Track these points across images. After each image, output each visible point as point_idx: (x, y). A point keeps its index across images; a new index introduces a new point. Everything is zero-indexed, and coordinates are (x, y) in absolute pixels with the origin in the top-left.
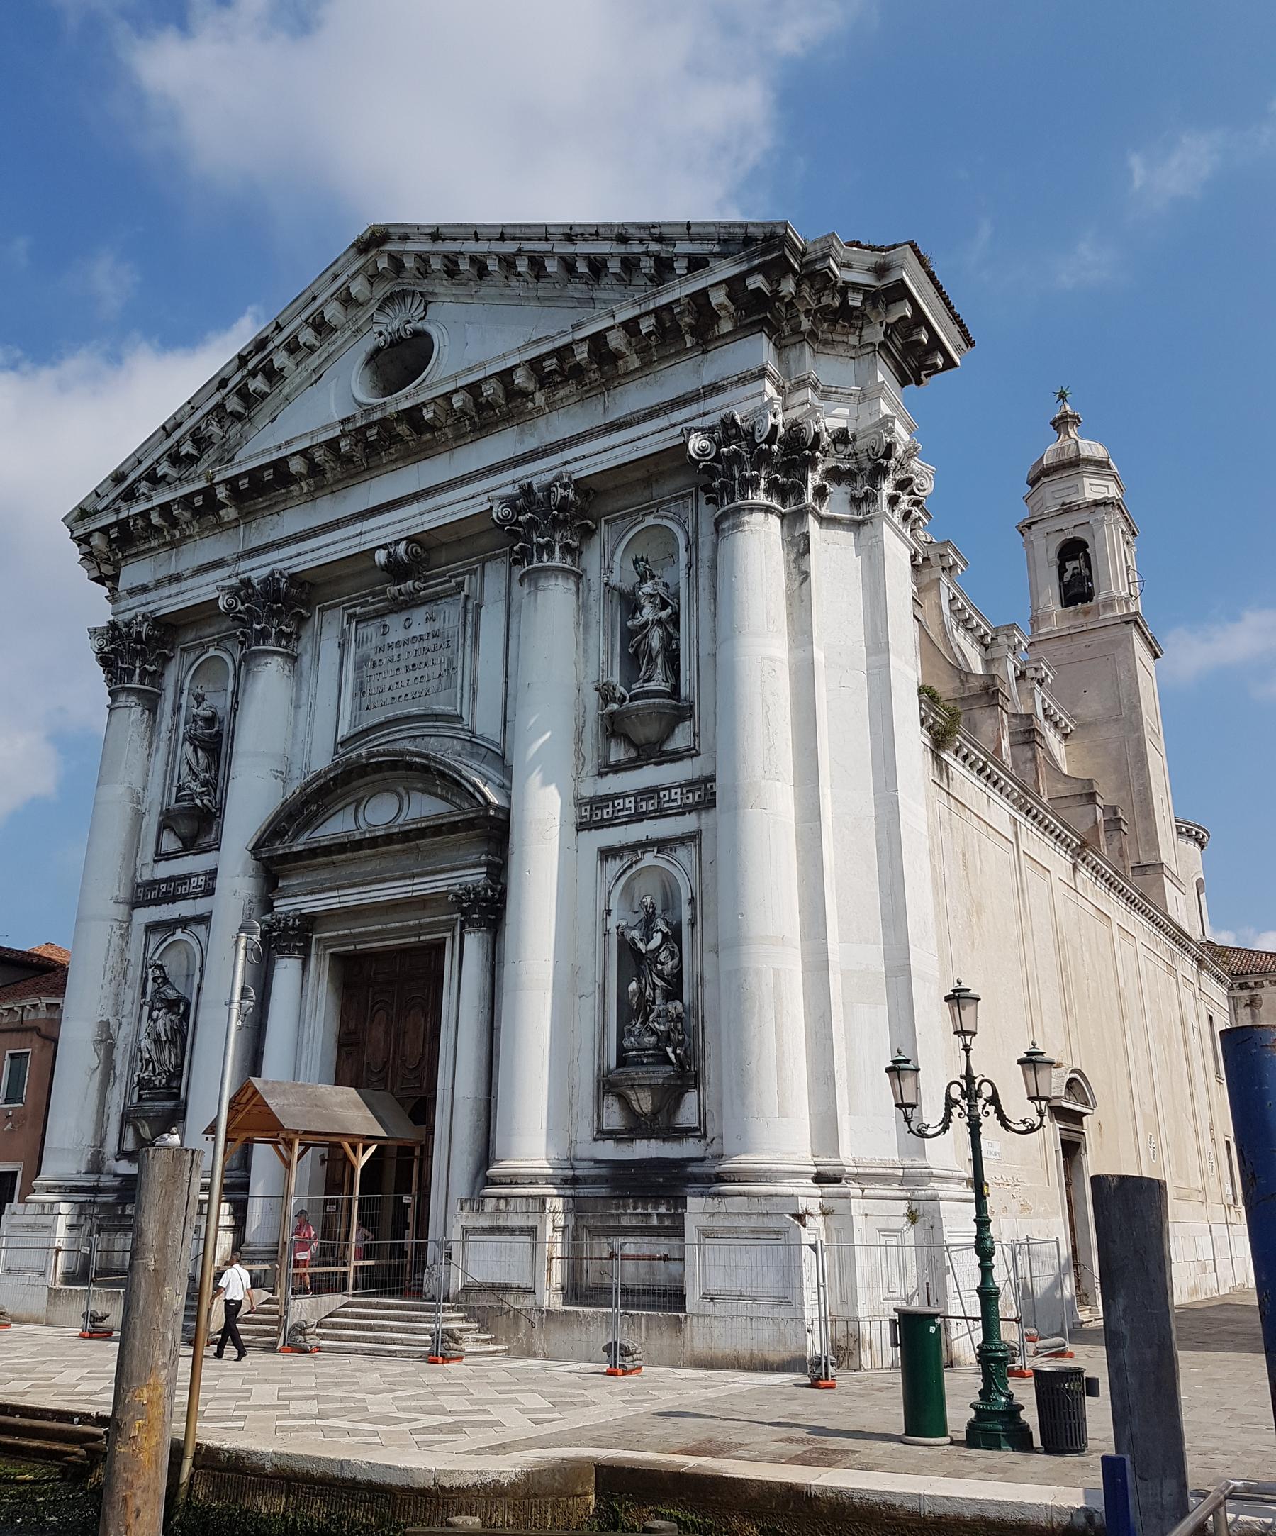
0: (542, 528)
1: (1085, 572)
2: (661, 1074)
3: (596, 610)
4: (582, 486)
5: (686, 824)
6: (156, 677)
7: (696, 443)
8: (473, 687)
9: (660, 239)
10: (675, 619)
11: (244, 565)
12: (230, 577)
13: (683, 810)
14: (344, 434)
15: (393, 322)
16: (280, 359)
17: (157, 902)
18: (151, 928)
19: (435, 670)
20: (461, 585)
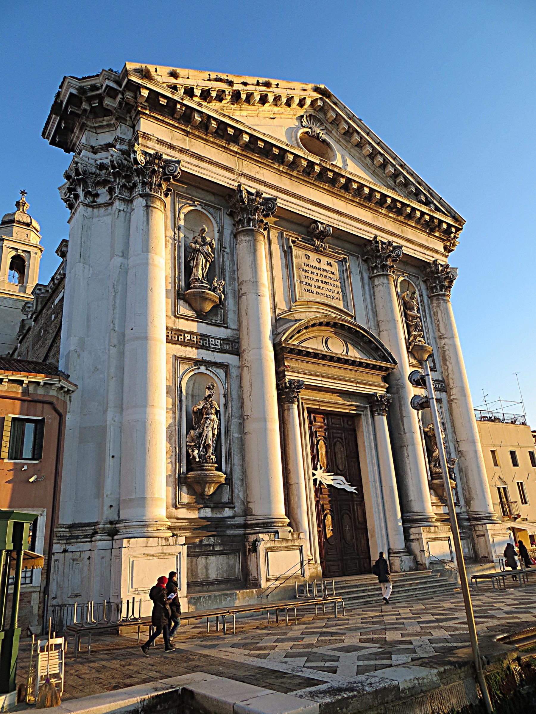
9: (431, 194)
12: (234, 180)
14: (320, 164)
16: (271, 98)
17: (183, 344)
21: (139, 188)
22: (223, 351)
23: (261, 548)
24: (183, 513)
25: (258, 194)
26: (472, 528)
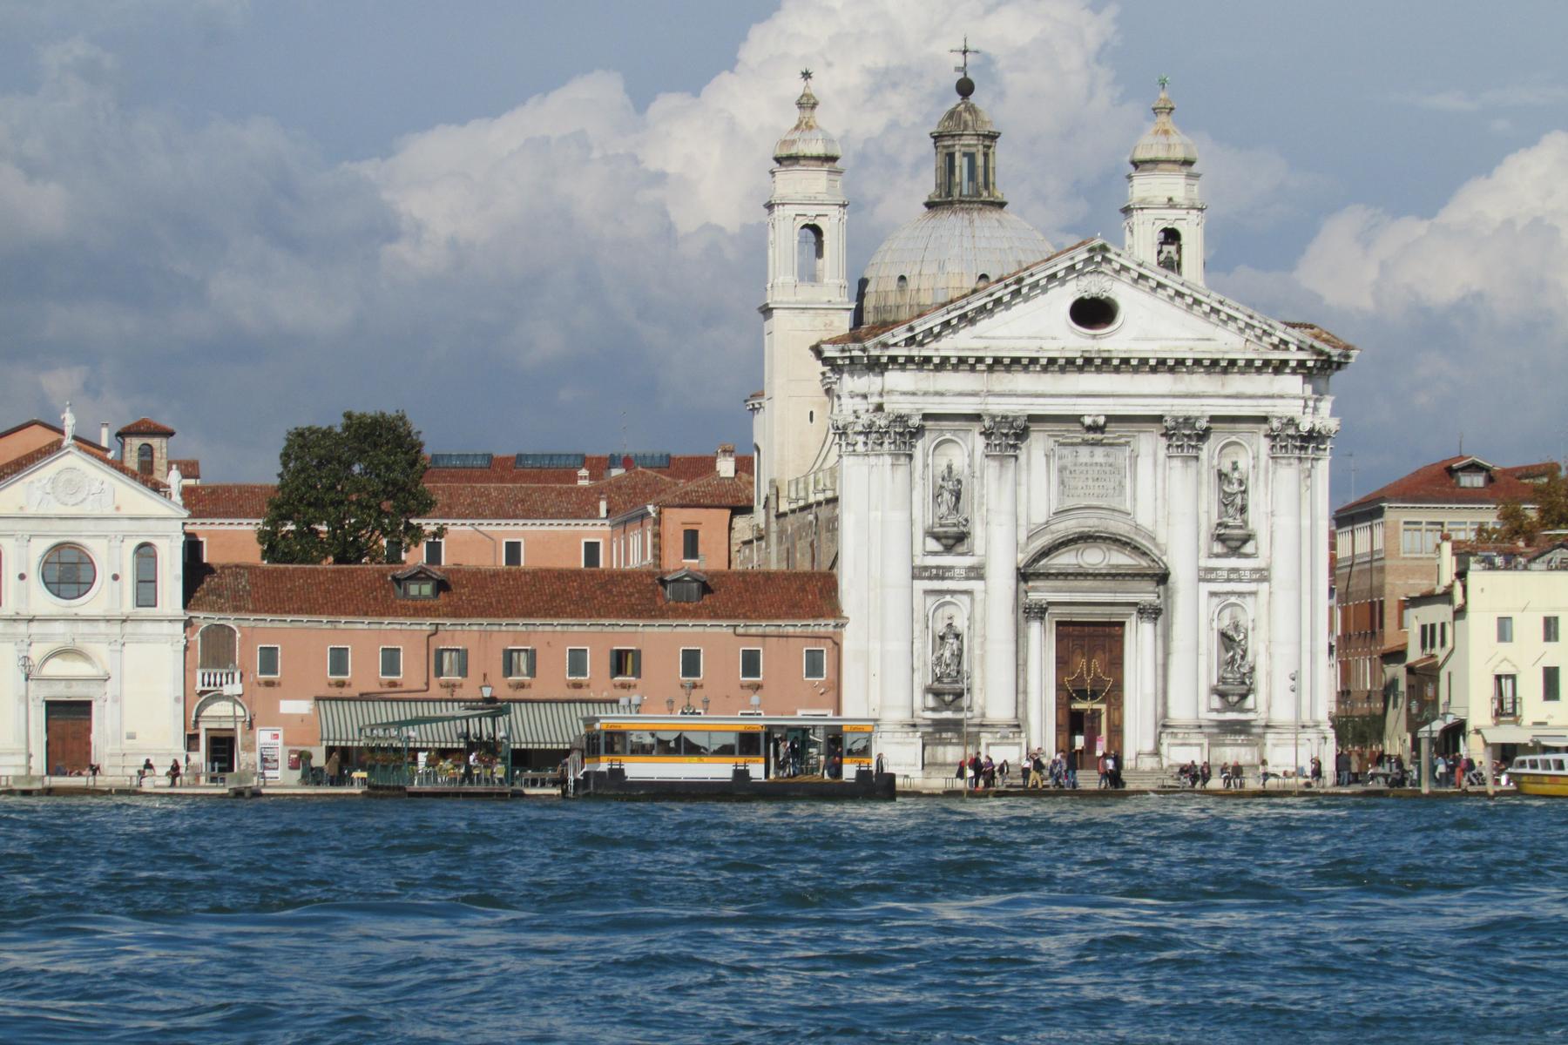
0: (1186, 435)
1: (1176, 258)
2: (1242, 689)
3: (1205, 476)
4: (1213, 419)
5: (1252, 587)
6: (912, 446)
7: (1275, 424)
8: (1135, 499)
10: (1244, 492)
11: (990, 400)
13: (1251, 581)
15: (1090, 286)
16: (1025, 290)
17: (930, 578)
18: (927, 592)
19: (1112, 485)
20: (1127, 443)
21: (886, 445)
22: (968, 578)
23: (983, 742)
24: (929, 715)
25: (1005, 417)
26: (1262, 736)
